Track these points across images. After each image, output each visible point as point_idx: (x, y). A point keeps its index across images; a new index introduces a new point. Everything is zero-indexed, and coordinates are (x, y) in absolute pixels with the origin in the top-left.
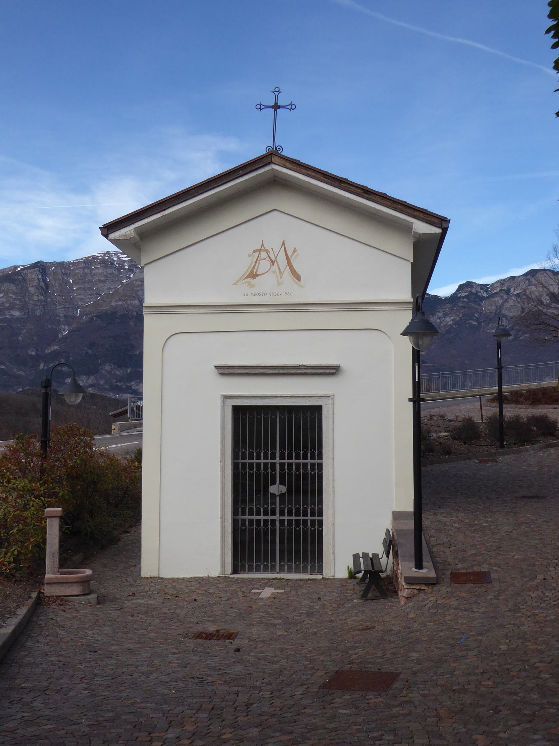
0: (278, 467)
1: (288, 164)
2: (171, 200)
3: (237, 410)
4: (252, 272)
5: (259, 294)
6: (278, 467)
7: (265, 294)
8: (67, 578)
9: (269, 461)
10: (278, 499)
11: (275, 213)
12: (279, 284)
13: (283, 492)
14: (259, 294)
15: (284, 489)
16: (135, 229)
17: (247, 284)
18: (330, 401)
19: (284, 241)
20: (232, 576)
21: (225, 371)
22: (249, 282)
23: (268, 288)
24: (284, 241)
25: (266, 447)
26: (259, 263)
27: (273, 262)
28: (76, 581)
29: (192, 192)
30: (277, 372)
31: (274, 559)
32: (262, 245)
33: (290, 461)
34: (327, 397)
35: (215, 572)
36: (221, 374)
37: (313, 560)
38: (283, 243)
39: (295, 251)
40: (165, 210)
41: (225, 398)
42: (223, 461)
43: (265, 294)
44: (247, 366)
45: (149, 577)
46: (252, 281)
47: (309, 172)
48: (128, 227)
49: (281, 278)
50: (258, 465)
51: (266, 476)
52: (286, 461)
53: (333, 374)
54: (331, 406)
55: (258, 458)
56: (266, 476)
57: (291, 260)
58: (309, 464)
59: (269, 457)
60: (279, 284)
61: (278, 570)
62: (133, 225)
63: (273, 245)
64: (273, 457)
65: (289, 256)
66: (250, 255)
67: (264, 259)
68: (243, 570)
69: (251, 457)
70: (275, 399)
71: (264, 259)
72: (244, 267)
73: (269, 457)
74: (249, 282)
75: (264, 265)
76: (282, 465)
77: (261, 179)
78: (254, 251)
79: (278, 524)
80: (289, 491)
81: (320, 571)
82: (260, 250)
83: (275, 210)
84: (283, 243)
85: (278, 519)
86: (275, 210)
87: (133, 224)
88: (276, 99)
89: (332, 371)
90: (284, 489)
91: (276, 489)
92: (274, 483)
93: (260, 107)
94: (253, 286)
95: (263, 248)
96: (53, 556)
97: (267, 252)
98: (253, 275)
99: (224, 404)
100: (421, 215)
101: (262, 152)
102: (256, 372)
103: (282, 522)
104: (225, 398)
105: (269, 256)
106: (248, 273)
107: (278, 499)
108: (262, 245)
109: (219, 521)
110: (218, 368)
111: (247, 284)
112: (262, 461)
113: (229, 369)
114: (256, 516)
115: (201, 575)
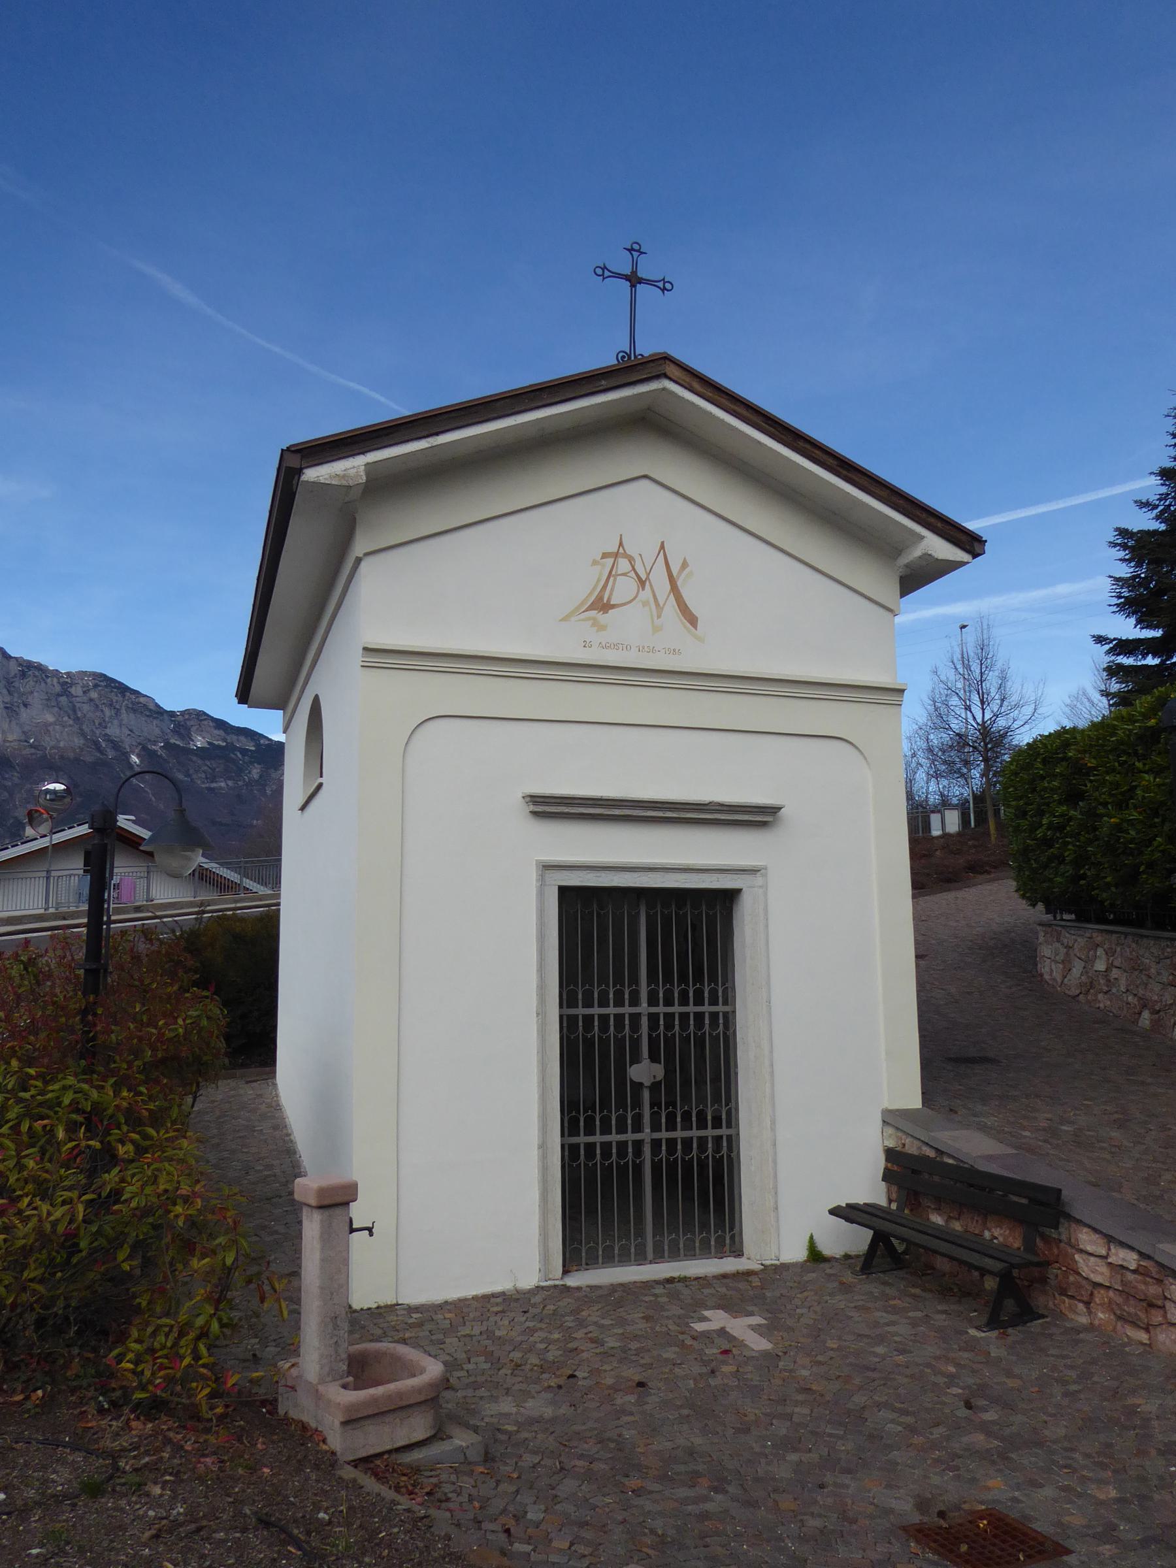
0: (644, 1021)
1: (696, 385)
2: (453, 414)
3: (565, 892)
4: (600, 598)
5: (616, 646)
6: (644, 1021)
7: (628, 648)
8: (400, 1395)
9: (627, 1010)
10: (646, 1095)
11: (645, 483)
12: (656, 629)
13: (658, 1079)
14: (616, 646)
15: (659, 1071)
16: (367, 464)
17: (590, 622)
18: (758, 880)
19: (663, 543)
20: (573, 1281)
21: (550, 808)
22: (594, 619)
23: (633, 634)
24: (663, 543)
25: (619, 980)
26: (615, 580)
27: (642, 583)
28: (422, 1398)
29: (499, 404)
30: (660, 814)
31: (640, 1233)
32: (621, 544)
33: (669, 1010)
34: (753, 871)
35: (529, 1279)
36: (534, 813)
37: (720, 1225)
38: (662, 546)
39: (685, 565)
40: (437, 434)
41: (547, 867)
42: (541, 1014)
43: (628, 648)
44: (601, 800)
45: (375, 1306)
46: (602, 617)
47: (736, 408)
48: (351, 459)
49: (659, 617)
50: (604, 1019)
51: (620, 1044)
52: (661, 1009)
53: (763, 824)
54: (761, 891)
55: (603, 1003)
56: (620, 1044)
57: (679, 583)
58: (707, 1015)
59: (627, 1002)
60: (656, 629)
61: (650, 1256)
62: (362, 457)
63: (642, 546)
64: (635, 1002)
65: (675, 574)
66: (595, 563)
67: (624, 574)
68: (592, 1262)
69: (588, 1004)
70: (651, 875)
71: (624, 574)
72: (584, 584)
73: (627, 1002)
74: (594, 619)
75: (624, 588)
76: (653, 1018)
77: (630, 405)
78: (605, 556)
79: (647, 1150)
80: (669, 1072)
81: (739, 1253)
82: (616, 555)
83: (645, 477)
84: (662, 546)
85: (648, 1140)
86: (645, 477)
87: (363, 453)
88: (635, 264)
89: (759, 817)
90: (659, 1071)
91: (644, 1072)
92: (636, 1059)
93: (604, 272)
94: (602, 628)
95: (621, 550)
96: (336, 1327)
97: (631, 560)
98: (602, 605)
99: (542, 880)
100: (939, 525)
101: (610, 361)
102: (617, 812)
103: (656, 1144)
104: (547, 867)
105: (634, 569)
106: (593, 598)
107: (646, 1095)
108: (621, 544)
109: (535, 1153)
110: (534, 799)
111: (590, 622)
112: (611, 1010)
113: (559, 804)
114: (617, 1133)
115: (498, 1288)
